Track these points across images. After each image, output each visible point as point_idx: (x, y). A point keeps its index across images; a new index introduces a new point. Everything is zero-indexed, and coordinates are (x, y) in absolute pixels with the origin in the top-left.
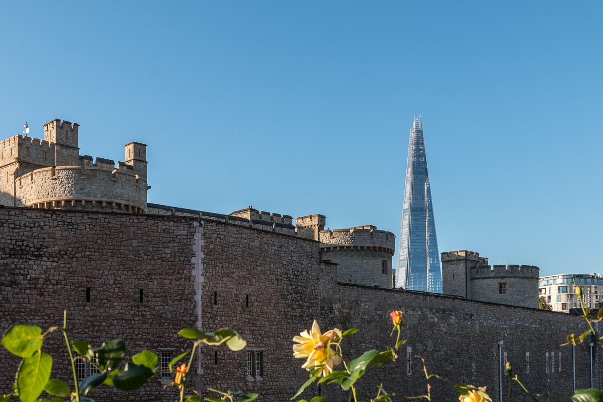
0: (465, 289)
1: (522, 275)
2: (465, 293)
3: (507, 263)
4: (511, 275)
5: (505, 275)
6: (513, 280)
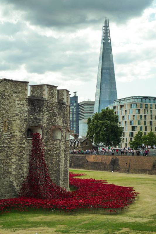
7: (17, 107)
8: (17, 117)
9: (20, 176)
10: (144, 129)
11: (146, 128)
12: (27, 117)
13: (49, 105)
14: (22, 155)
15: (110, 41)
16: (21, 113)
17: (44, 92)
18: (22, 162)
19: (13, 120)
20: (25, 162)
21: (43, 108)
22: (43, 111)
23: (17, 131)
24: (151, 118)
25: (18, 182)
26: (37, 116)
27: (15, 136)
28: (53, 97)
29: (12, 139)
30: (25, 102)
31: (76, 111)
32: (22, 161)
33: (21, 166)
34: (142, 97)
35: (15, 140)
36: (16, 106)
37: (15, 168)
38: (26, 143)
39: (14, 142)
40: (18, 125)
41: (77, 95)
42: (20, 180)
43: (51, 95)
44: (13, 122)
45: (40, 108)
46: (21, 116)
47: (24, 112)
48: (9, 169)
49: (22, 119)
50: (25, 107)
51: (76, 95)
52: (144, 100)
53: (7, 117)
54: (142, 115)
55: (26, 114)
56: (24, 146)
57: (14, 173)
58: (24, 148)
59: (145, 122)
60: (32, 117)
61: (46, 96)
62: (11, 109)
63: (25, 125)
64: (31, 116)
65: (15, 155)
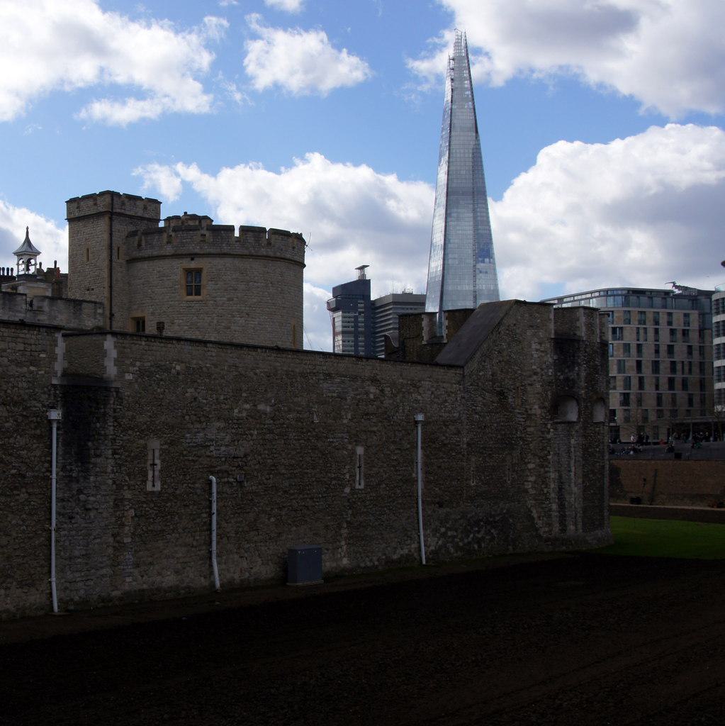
0: (106, 284)
2: (106, 294)
4: (212, 251)
5: (197, 250)
7: (535, 356)
8: (535, 377)
10: (635, 382)
11: (641, 380)
12: (552, 378)
13: (587, 350)
18: (546, 469)
19: (529, 384)
21: (579, 357)
22: (579, 365)
23: (536, 407)
24: (657, 351)
25: (540, 510)
26: (569, 374)
27: (533, 417)
28: (593, 333)
29: (528, 423)
31: (366, 327)
32: (547, 466)
36: (532, 356)
37: (535, 482)
38: (551, 430)
39: (532, 429)
40: (538, 393)
41: (369, 274)
42: (544, 506)
43: (590, 326)
44: (529, 388)
45: (574, 356)
46: (542, 375)
48: (526, 483)
50: (549, 356)
51: (364, 275)
53: (520, 378)
54: (629, 344)
55: (551, 370)
56: (549, 436)
57: (532, 492)
58: (549, 440)
59: (639, 364)
60: (562, 377)
61: (582, 332)
63: (549, 393)
64: (559, 374)
65: (534, 455)
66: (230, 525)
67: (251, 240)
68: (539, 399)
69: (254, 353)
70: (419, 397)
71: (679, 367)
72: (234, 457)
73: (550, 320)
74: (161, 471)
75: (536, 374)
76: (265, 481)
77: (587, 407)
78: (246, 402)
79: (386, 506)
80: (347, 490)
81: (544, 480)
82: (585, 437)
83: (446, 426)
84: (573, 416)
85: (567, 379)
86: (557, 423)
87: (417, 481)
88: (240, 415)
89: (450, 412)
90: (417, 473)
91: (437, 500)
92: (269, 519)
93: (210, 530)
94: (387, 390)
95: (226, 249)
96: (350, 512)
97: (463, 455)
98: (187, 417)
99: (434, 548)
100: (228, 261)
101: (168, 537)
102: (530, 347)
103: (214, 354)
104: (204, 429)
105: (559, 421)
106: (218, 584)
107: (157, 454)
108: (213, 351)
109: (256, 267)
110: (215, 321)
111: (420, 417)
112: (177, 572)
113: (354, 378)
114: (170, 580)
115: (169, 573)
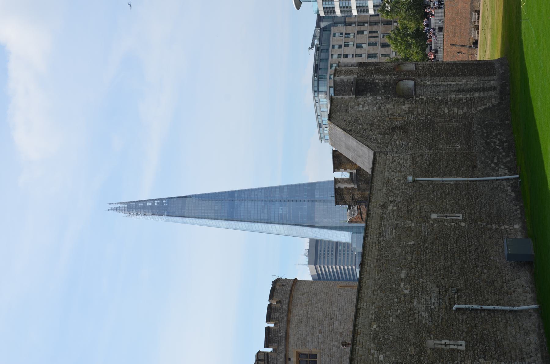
1: (284, 323)
3: (261, 324)
4: (283, 344)
5: (282, 355)
6: (292, 340)
7: (367, 108)
8: (382, 108)
9: (469, 102)
12: (383, 97)
14: (439, 101)
15: (164, 199)
16: (377, 103)
17: (345, 80)
20: (449, 97)
21: (369, 80)
22: (373, 80)
23: (403, 107)
26: (381, 86)
30: (360, 100)
33: (455, 101)
34: (314, 76)
35: (416, 109)
36: (367, 110)
37: (458, 108)
38: (420, 97)
39: (420, 110)
40: (394, 106)
42: (476, 102)
43: (347, 73)
44: (390, 112)
45: (368, 83)
47: (376, 99)
49: (385, 102)
52: (321, 72)
55: (378, 98)
56: (425, 99)
57: (465, 109)
58: (427, 98)
60: (383, 91)
62: (371, 114)
63: (394, 99)
64: (380, 92)
65: (438, 108)
66: (490, 298)
67: (277, 315)
68: (398, 105)
69: (365, 279)
70: (396, 179)
71: (373, 40)
72: (439, 293)
73: (342, 98)
74: (450, 340)
75: (380, 108)
76: (457, 275)
77: (404, 75)
78: (399, 285)
79: (475, 201)
80: (463, 224)
81: (457, 102)
82: (425, 76)
83: (416, 163)
84: (411, 83)
85: (384, 87)
86: (415, 93)
87: (456, 181)
88: (409, 289)
89: (406, 161)
90: (451, 181)
91: (470, 169)
92: (485, 274)
93: (494, 311)
94: (390, 199)
95: (283, 334)
96: (479, 223)
97: (438, 152)
98: (411, 322)
99: (507, 171)
100: (292, 332)
101: (499, 337)
102: (361, 111)
103: (365, 304)
104: (419, 312)
105: (414, 92)
106: (535, 306)
107: (438, 342)
108: (363, 304)
109: (297, 312)
110: (336, 343)
111: (410, 178)
112: (528, 333)
113: (382, 219)
114: (533, 338)
115: (528, 339)
